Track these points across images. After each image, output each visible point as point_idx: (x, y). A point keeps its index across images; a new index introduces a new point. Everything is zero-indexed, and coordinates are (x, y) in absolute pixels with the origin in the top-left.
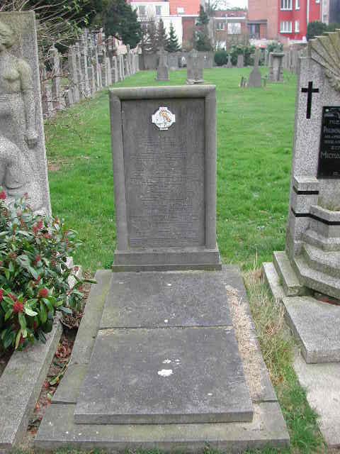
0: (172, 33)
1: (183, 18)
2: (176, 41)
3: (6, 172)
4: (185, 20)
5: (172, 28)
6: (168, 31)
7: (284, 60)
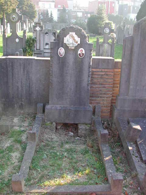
0: (51, 15)
1: (58, 9)
2: (53, 18)
4: (59, 10)
5: (51, 13)
6: (50, 14)
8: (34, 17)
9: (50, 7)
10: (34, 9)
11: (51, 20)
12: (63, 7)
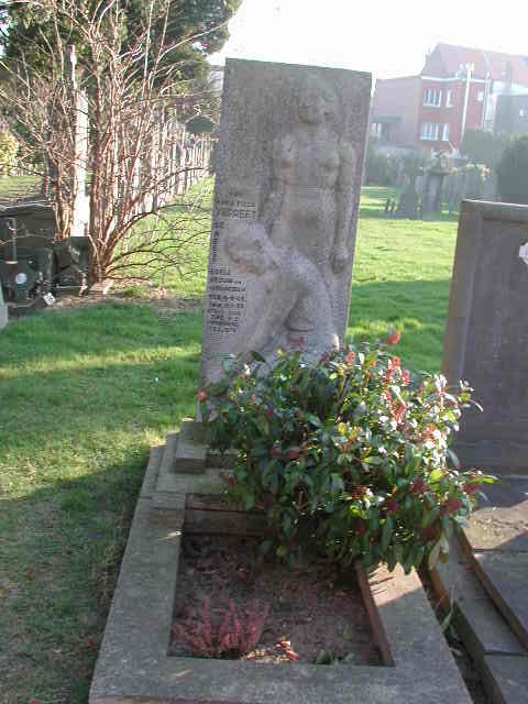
3: (298, 305)
7: (445, 177)
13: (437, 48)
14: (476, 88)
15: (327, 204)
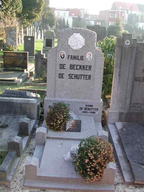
0: (67, 23)
4: (73, 18)
5: (67, 21)
6: (66, 22)
8: (54, 25)
9: (65, 15)
10: (53, 18)
11: (67, 26)
12: (78, 16)
13: (114, 2)
14: (122, 13)
15: (14, 36)
